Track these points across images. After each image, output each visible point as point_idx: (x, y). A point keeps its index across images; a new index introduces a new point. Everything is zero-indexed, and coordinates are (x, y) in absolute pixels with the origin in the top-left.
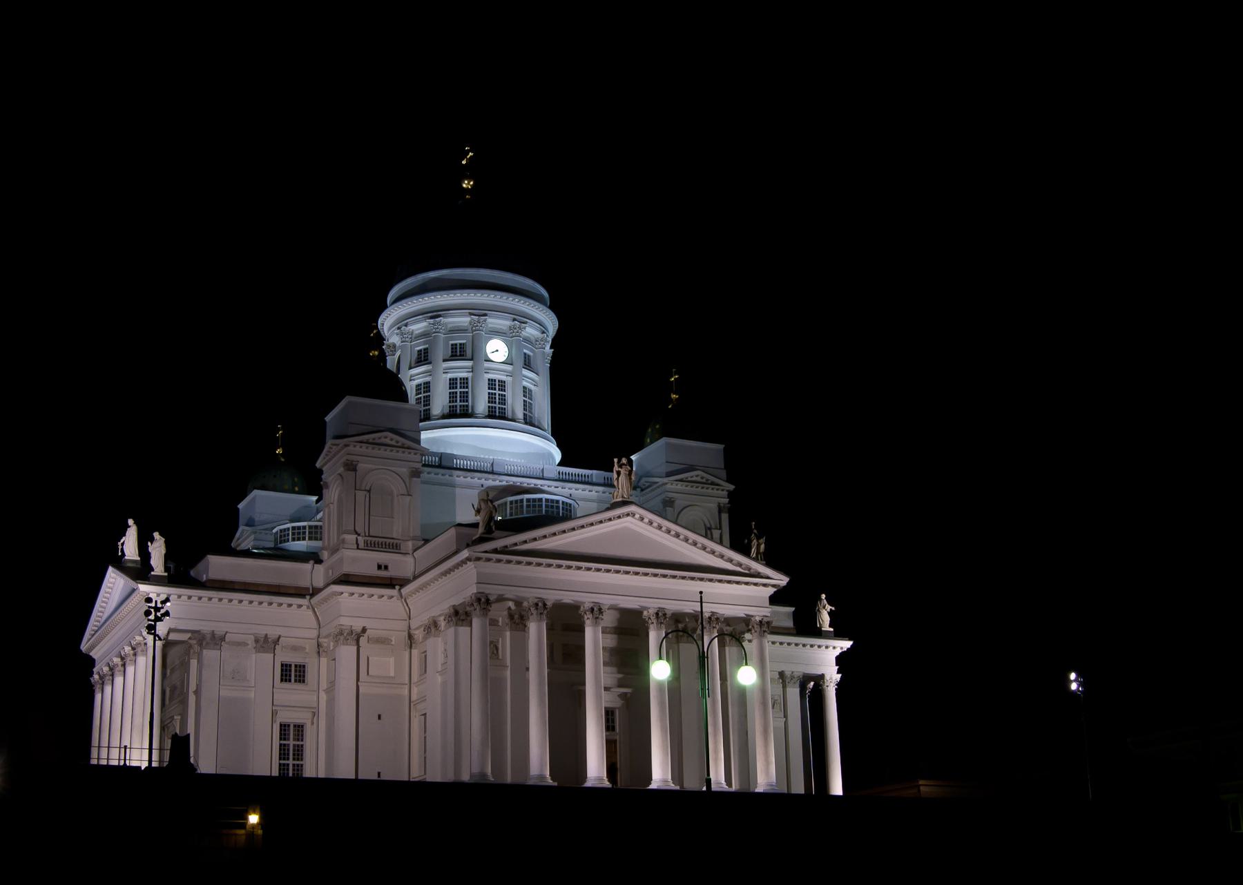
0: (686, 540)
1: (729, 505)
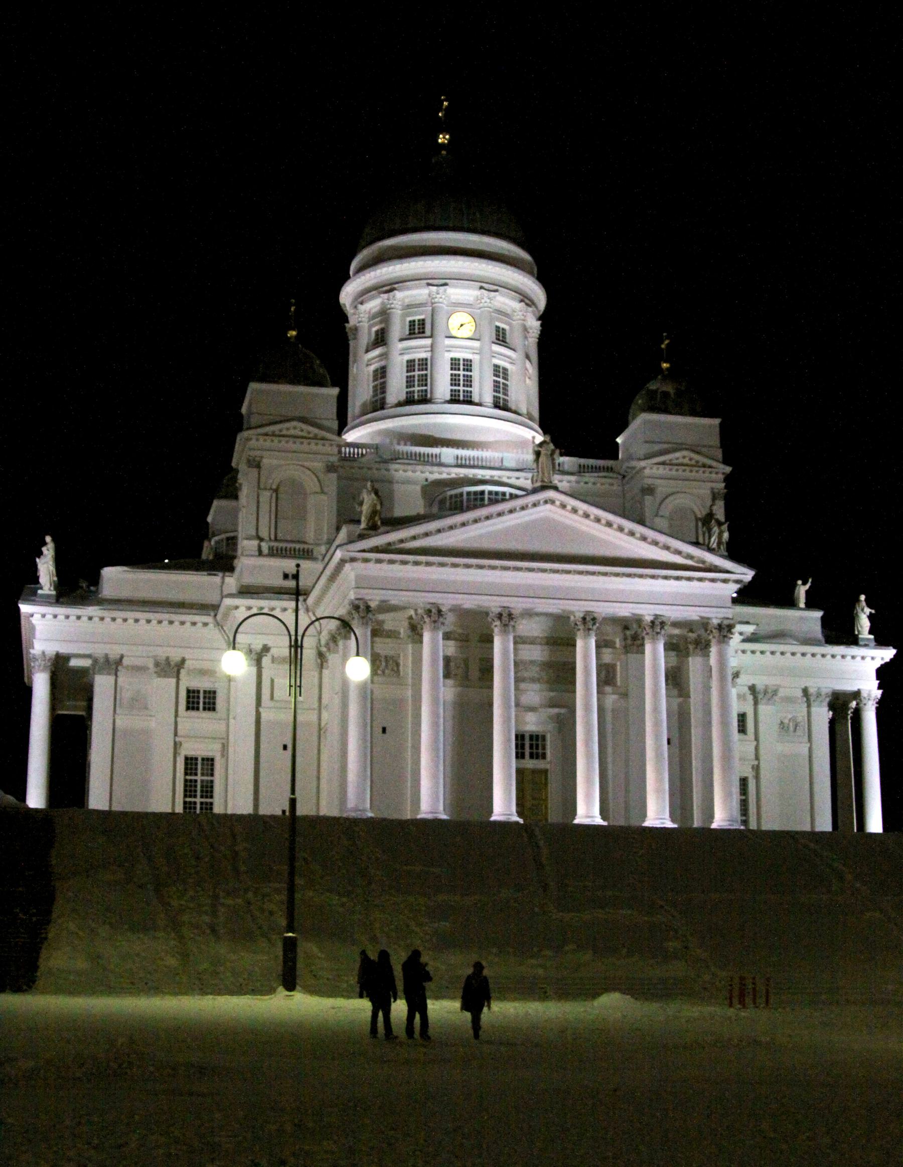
1: (726, 491)
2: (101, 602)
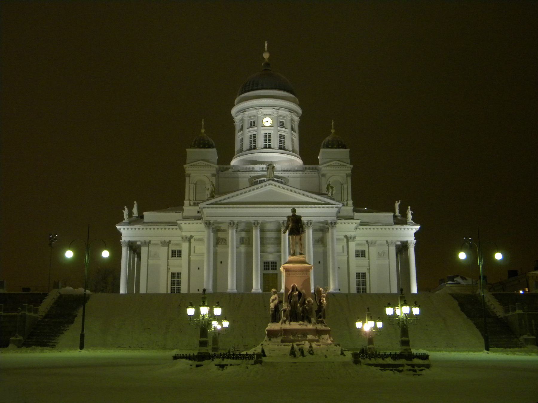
2: (144, 223)
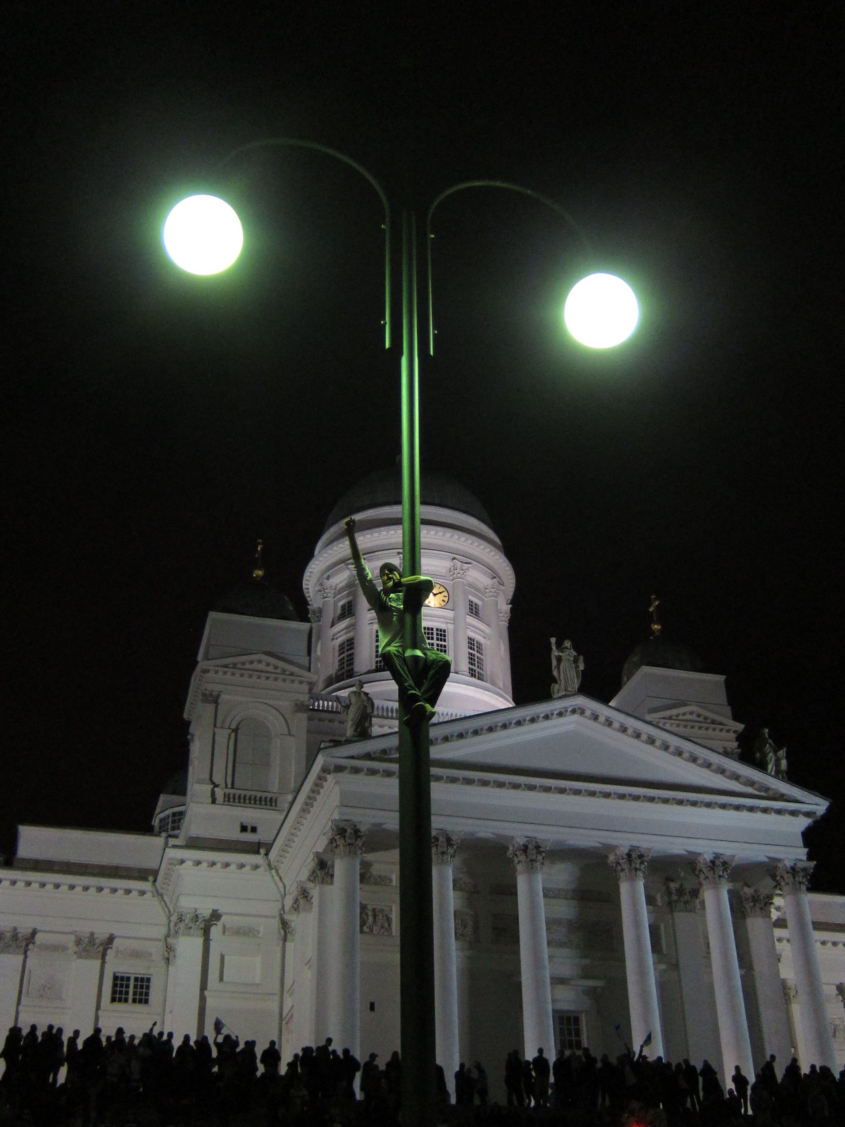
0: (666, 747)
1: (739, 750)
